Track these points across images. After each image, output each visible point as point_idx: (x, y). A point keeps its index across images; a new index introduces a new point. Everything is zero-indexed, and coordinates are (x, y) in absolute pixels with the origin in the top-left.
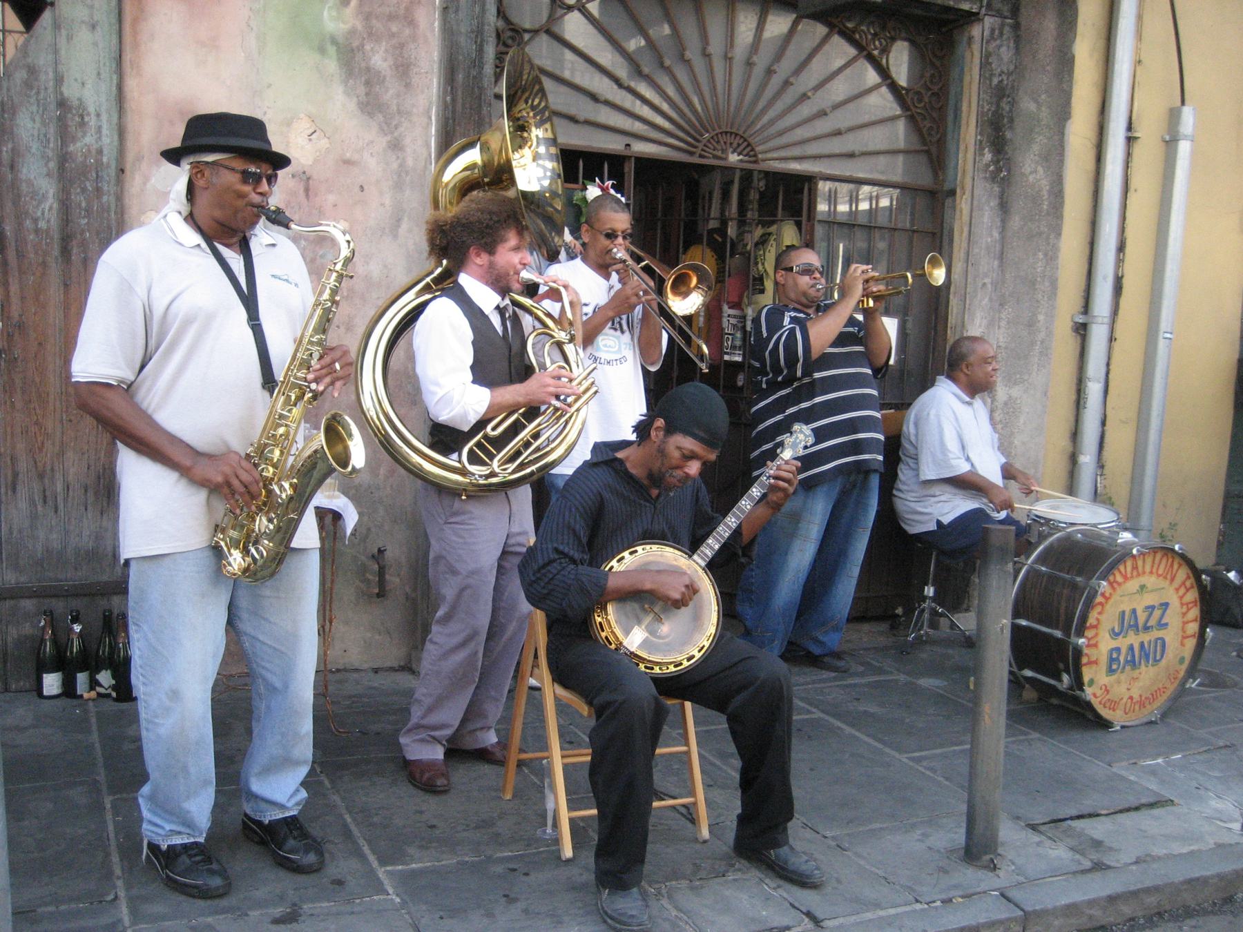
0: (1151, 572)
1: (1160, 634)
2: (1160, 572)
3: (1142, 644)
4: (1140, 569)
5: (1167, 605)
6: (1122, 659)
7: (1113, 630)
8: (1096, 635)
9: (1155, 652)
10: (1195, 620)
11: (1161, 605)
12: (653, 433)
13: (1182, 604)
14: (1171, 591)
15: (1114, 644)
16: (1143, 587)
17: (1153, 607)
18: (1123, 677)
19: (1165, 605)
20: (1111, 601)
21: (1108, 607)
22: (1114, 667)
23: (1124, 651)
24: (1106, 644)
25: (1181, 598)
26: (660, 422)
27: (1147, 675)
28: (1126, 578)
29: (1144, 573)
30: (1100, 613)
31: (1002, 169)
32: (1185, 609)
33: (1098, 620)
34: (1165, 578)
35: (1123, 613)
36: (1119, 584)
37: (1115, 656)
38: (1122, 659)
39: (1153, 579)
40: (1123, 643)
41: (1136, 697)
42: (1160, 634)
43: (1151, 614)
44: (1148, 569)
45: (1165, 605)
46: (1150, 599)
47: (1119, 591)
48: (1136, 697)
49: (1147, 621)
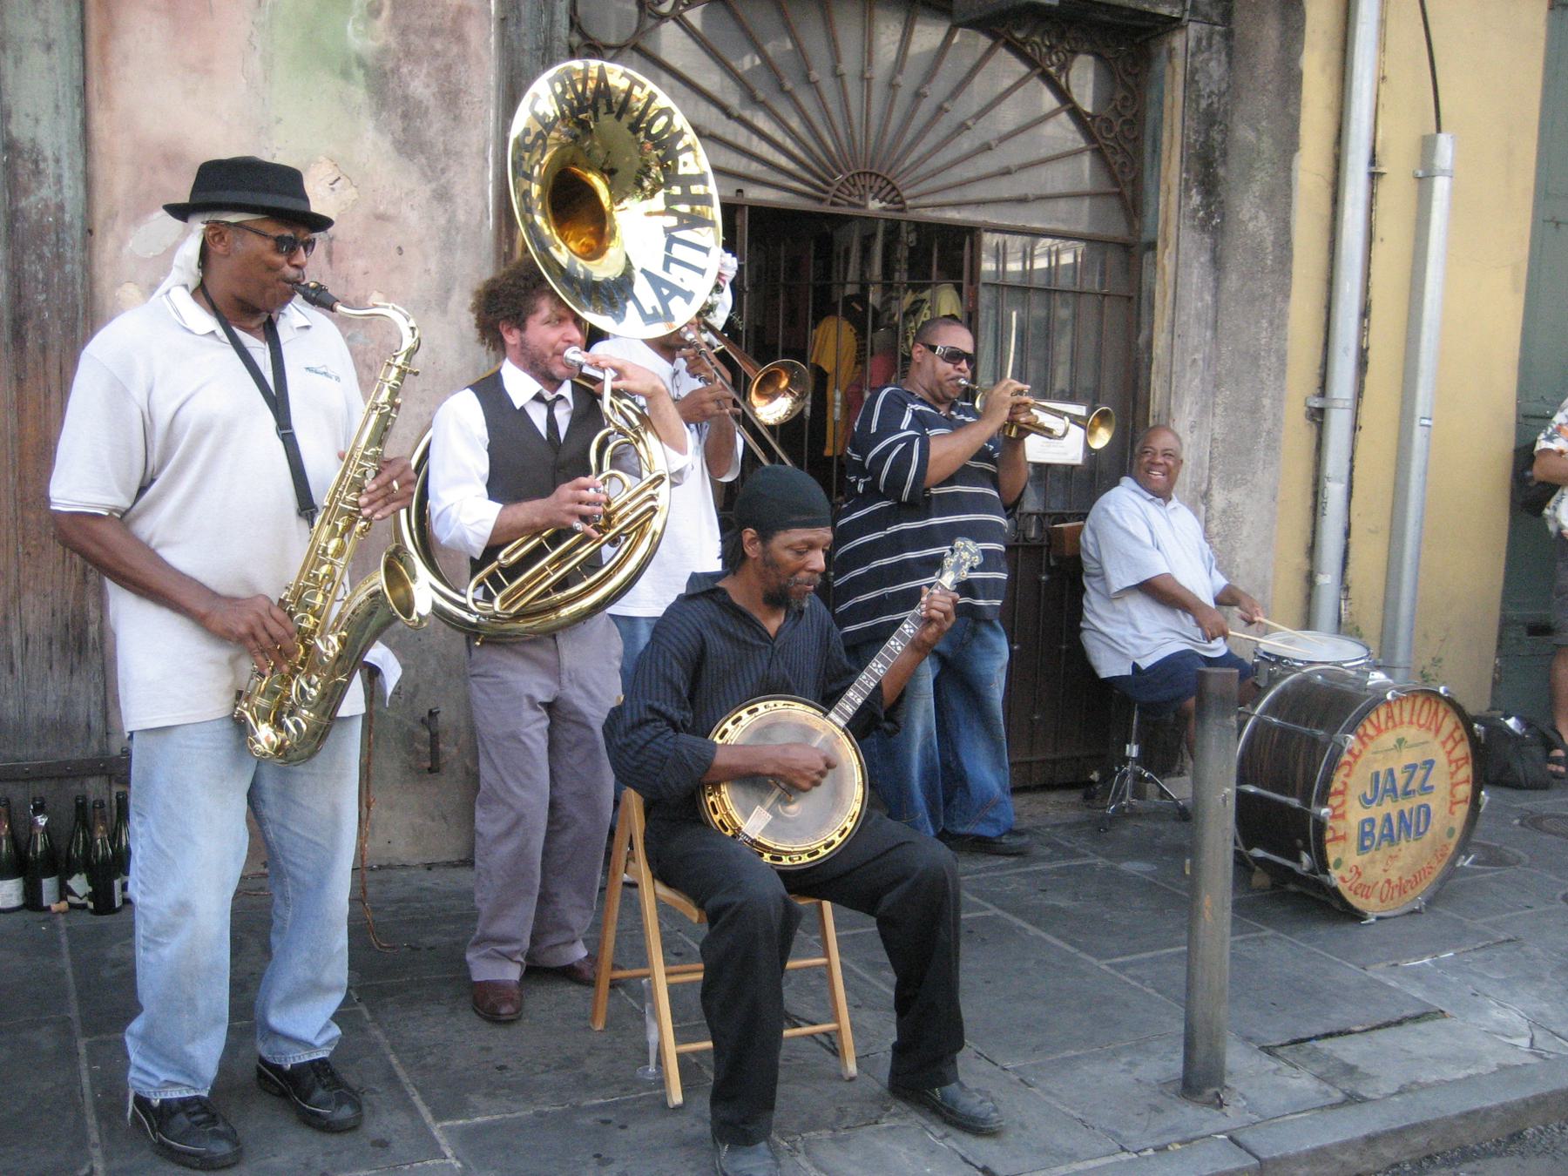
0: (1411, 722)
3: (1402, 814)
6: (1377, 832)
8: (1343, 803)
11: (1426, 763)
12: (749, 550)
13: (1450, 762)
14: (1436, 744)
15: (1366, 814)
16: (1400, 741)
17: (1414, 767)
18: (1379, 855)
19: (1430, 764)
20: (1360, 761)
21: (1357, 768)
22: (1367, 843)
23: (1379, 822)
24: (1356, 814)
25: (1449, 753)
26: (749, 533)
27: (1408, 851)
28: (1379, 730)
29: (1402, 723)
30: (1347, 775)
31: (1214, 215)
32: (1453, 767)
33: (1345, 784)
34: (1429, 729)
35: (1377, 775)
36: (1371, 738)
37: (1367, 829)
38: (1377, 832)
40: (1377, 812)
41: (1395, 880)
42: (1423, 800)
44: (1406, 718)
45: (1430, 764)
46: (1409, 757)
47: (1372, 746)
48: (1395, 880)
49: (1407, 784)
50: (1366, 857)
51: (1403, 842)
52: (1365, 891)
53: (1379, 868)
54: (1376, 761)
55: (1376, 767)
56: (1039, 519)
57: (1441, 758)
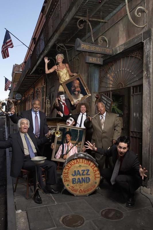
0: (82, 163)
1: (88, 176)
2: (85, 163)
3: (82, 178)
4: (79, 162)
5: (89, 170)
6: (77, 181)
7: (73, 174)
8: (68, 175)
9: (87, 180)
10: (99, 174)
11: (87, 170)
13: (94, 170)
14: (90, 167)
15: (73, 177)
16: (80, 166)
17: (84, 170)
18: (77, 185)
20: (71, 168)
22: (74, 182)
23: (77, 179)
24: (71, 177)
25: (93, 169)
27: (84, 185)
28: (75, 163)
29: (80, 163)
31: (94, 65)
32: (95, 171)
33: (68, 172)
34: (87, 164)
35: (75, 171)
36: (73, 165)
37: (74, 180)
38: (77, 181)
39: (83, 164)
40: (77, 177)
41: (82, 189)
42: (88, 176)
43: (84, 172)
44: (81, 161)
46: (83, 169)
50: (74, 185)
51: (83, 183)
52: (76, 191)
53: (78, 187)
54: (74, 168)
55: (75, 170)
56: (69, 169)
57: (91, 169)
